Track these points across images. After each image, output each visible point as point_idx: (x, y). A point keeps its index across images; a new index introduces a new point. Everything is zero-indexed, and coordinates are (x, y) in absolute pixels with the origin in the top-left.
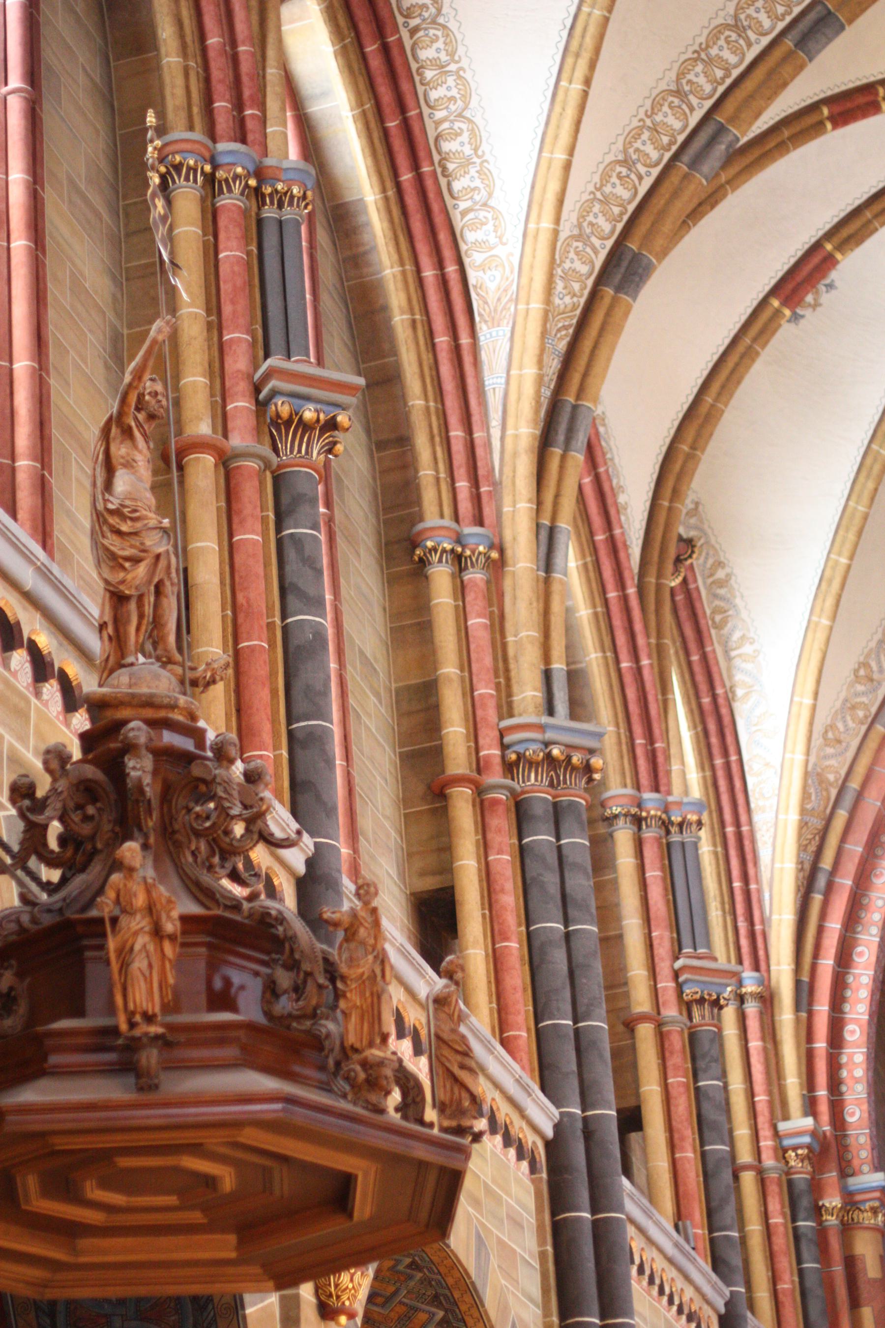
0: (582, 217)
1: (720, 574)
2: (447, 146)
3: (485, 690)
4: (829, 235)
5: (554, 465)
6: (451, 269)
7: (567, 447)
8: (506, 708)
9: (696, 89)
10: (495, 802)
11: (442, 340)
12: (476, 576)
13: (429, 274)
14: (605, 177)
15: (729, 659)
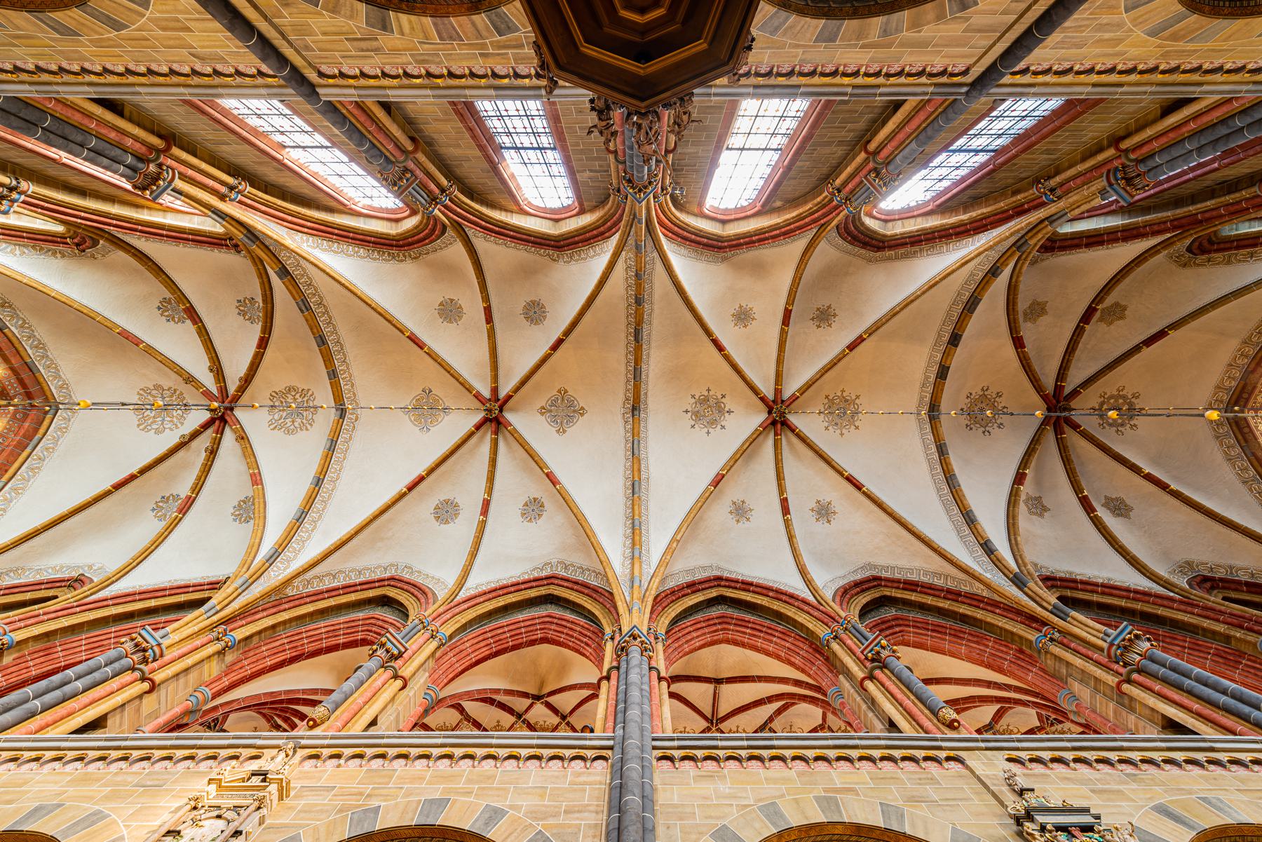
0: (303, 268)
1: (58, 255)
2: (336, 245)
3: (190, 172)
4: (203, 325)
5: (242, 229)
6: (306, 230)
7: (245, 235)
8: (183, 177)
9: (319, 308)
10: (151, 154)
11: (290, 218)
12: (223, 190)
13: (309, 224)
14: (309, 278)
15: (15, 245)
